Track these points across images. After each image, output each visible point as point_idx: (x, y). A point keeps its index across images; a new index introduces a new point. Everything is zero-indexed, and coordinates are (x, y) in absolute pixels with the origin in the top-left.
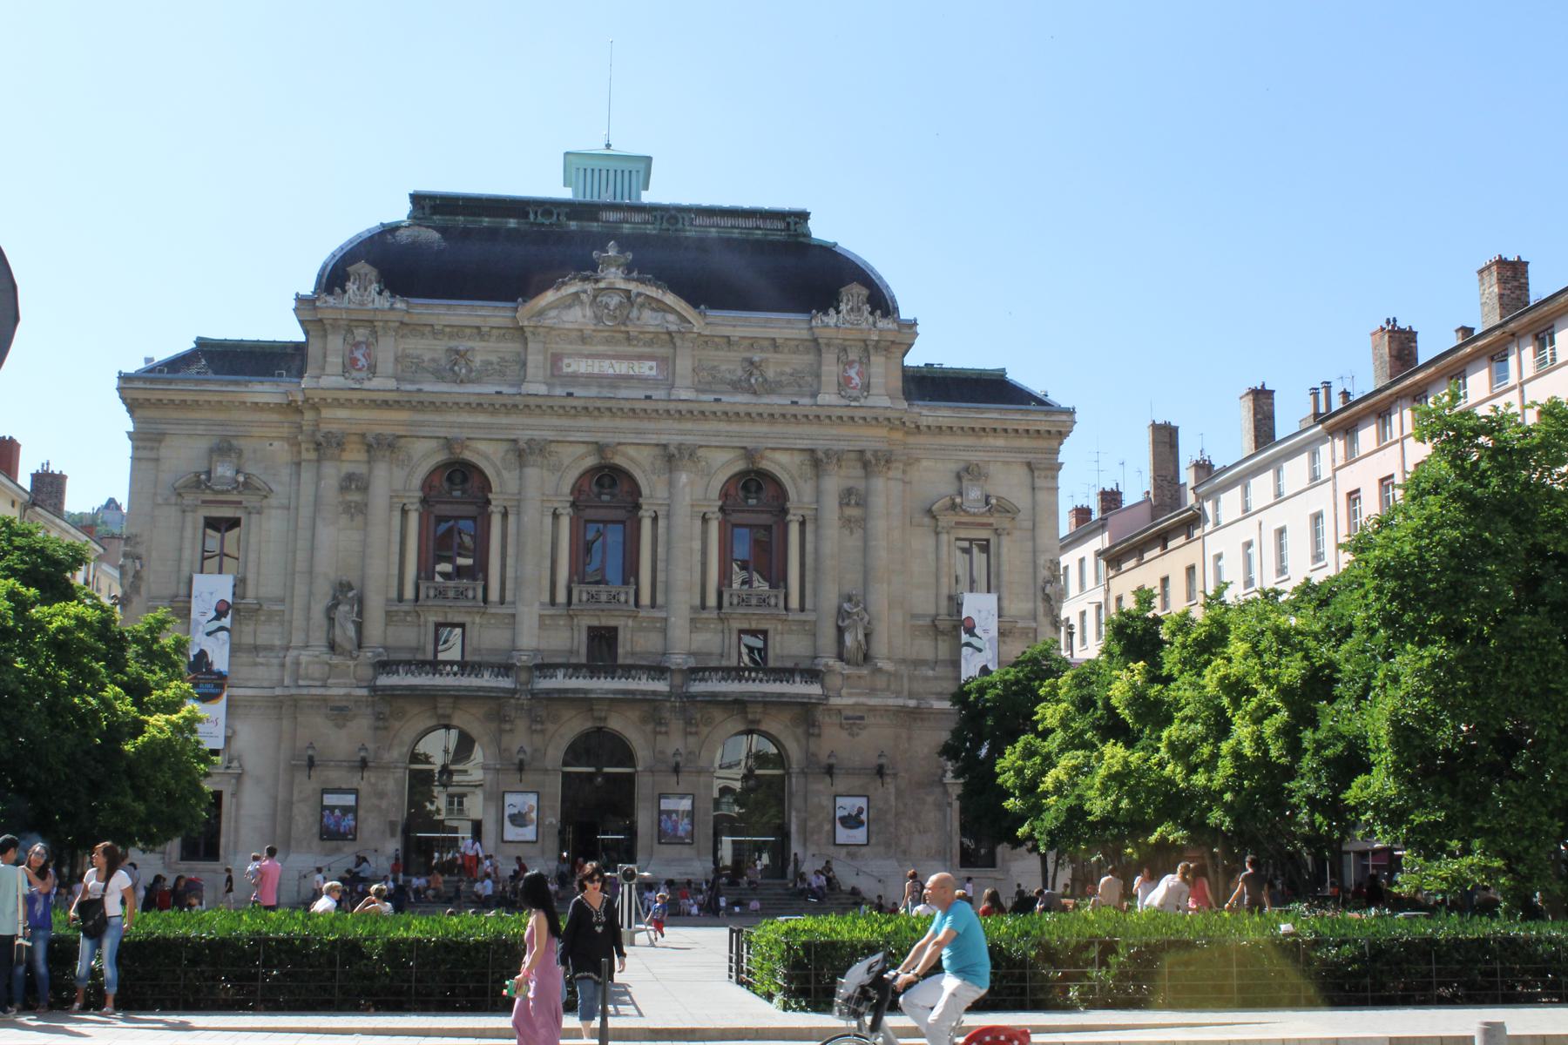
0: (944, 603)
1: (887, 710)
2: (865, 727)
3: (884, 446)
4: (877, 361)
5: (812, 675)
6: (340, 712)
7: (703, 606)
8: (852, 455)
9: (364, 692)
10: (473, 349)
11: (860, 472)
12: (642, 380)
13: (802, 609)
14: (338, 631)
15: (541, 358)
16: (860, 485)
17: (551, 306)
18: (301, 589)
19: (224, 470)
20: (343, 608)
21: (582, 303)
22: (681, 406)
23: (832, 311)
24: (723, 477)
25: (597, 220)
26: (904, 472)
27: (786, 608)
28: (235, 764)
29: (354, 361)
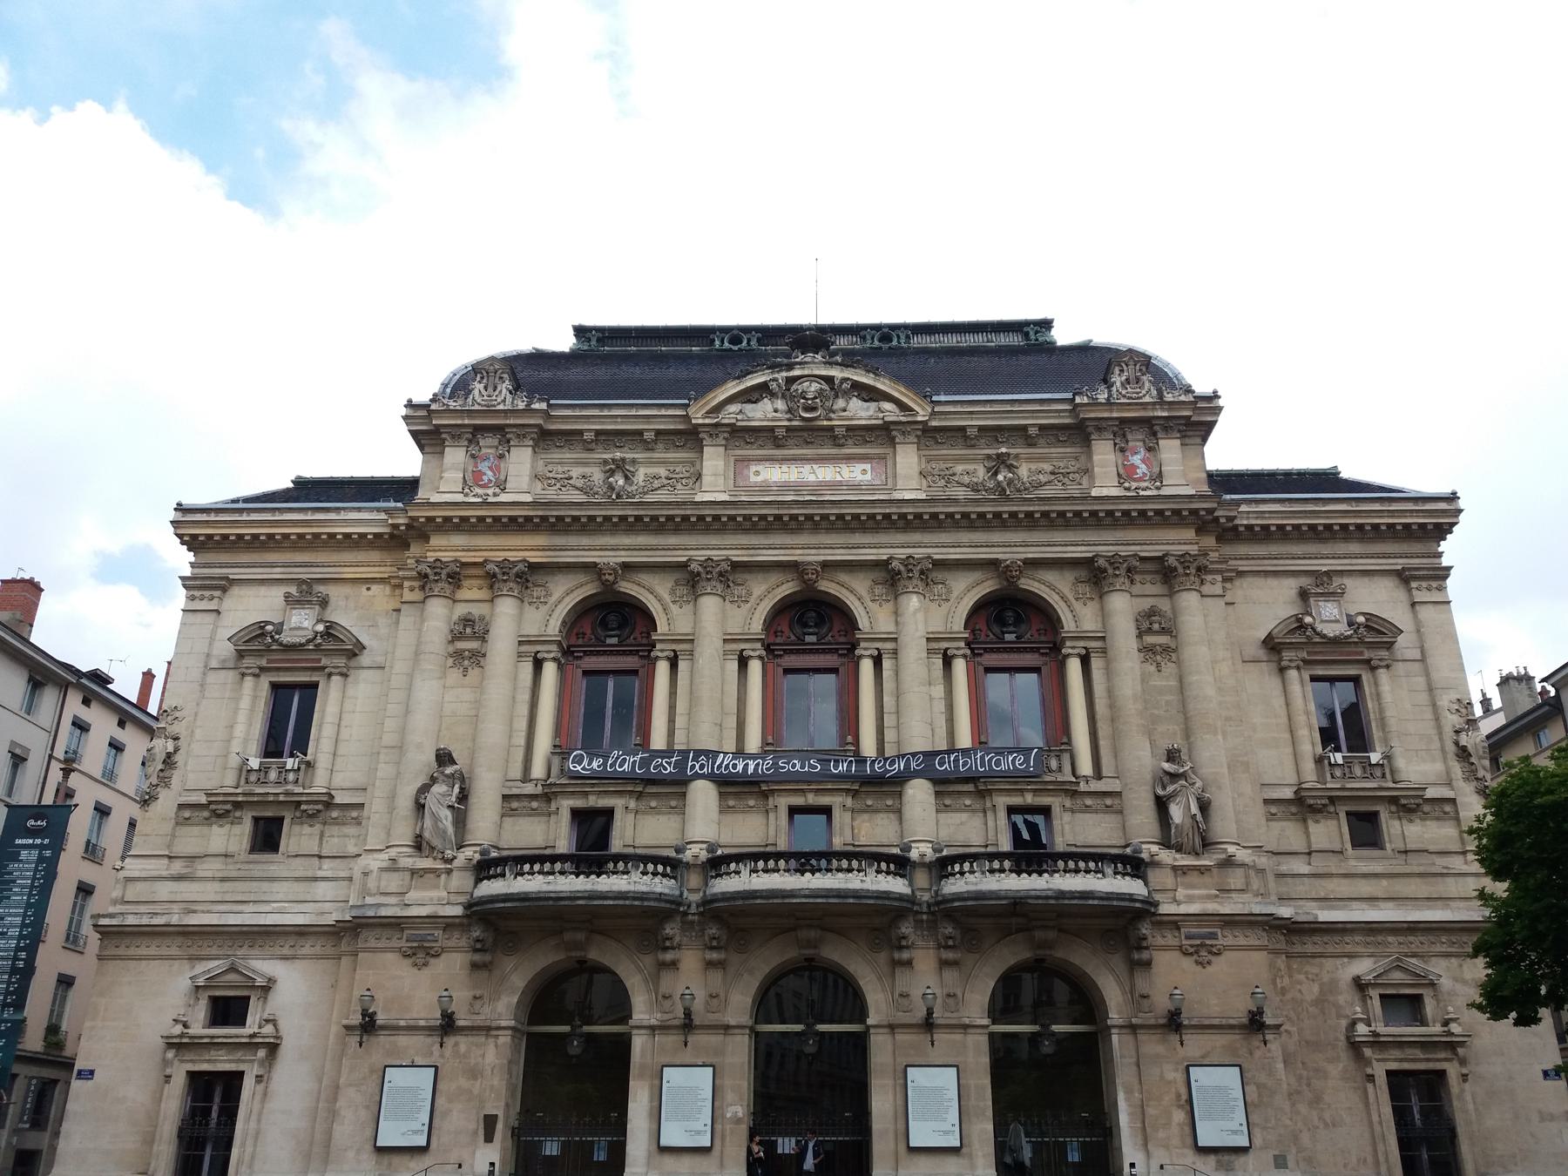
0: (1309, 767)
3: (1193, 549)
8: (1149, 566)
9: (458, 911)
10: (634, 461)
12: (855, 487)
13: (1098, 775)
14: (428, 822)
16: (1164, 605)
17: (731, 400)
18: (385, 770)
20: (439, 789)
29: (478, 475)
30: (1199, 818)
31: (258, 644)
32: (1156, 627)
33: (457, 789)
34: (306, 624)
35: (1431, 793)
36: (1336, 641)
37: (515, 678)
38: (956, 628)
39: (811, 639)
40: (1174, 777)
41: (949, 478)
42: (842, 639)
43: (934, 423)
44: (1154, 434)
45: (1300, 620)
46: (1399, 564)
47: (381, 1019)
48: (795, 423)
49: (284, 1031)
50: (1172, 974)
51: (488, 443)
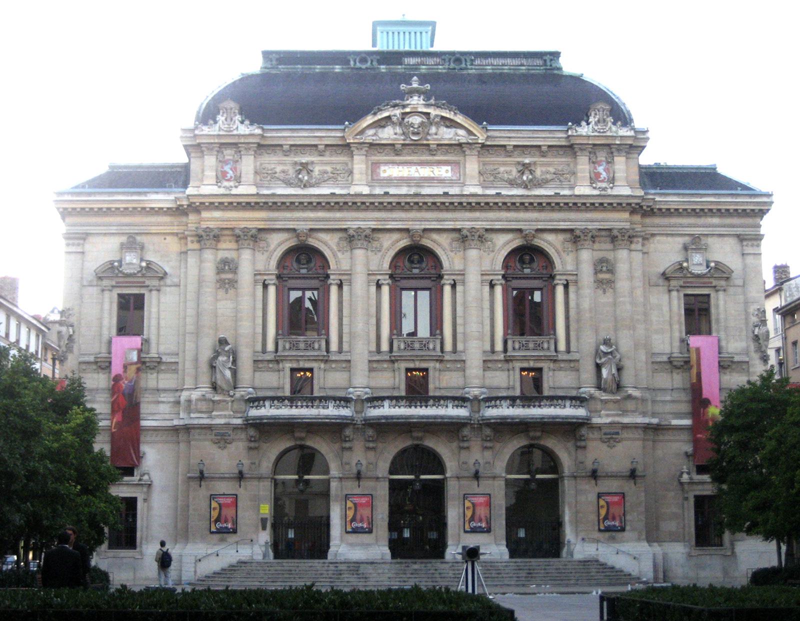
0: (677, 344)
1: (636, 426)
2: (619, 442)
3: (627, 225)
5: (579, 400)
6: (221, 436)
7: (493, 351)
8: (603, 233)
9: (239, 421)
10: (312, 163)
12: (441, 181)
13: (568, 351)
14: (218, 376)
15: (363, 166)
16: (610, 256)
17: (369, 127)
19: (131, 258)
20: (222, 359)
21: (393, 123)
23: (583, 123)
24: (505, 252)
25: (401, 64)
26: (643, 245)
27: (556, 350)
28: (146, 477)
29: (224, 174)
30: (616, 375)
31: (111, 272)
32: (604, 269)
33: (231, 358)
34: (134, 261)
35: (737, 359)
36: (698, 276)
37: (254, 295)
38: (497, 268)
40: (606, 354)
41: (495, 175)
42: (433, 271)
43: (488, 143)
44: (612, 153)
45: (681, 264)
46: (739, 231)
47: (205, 472)
48: (407, 142)
49: (153, 479)
50: (597, 452)
51: (229, 153)
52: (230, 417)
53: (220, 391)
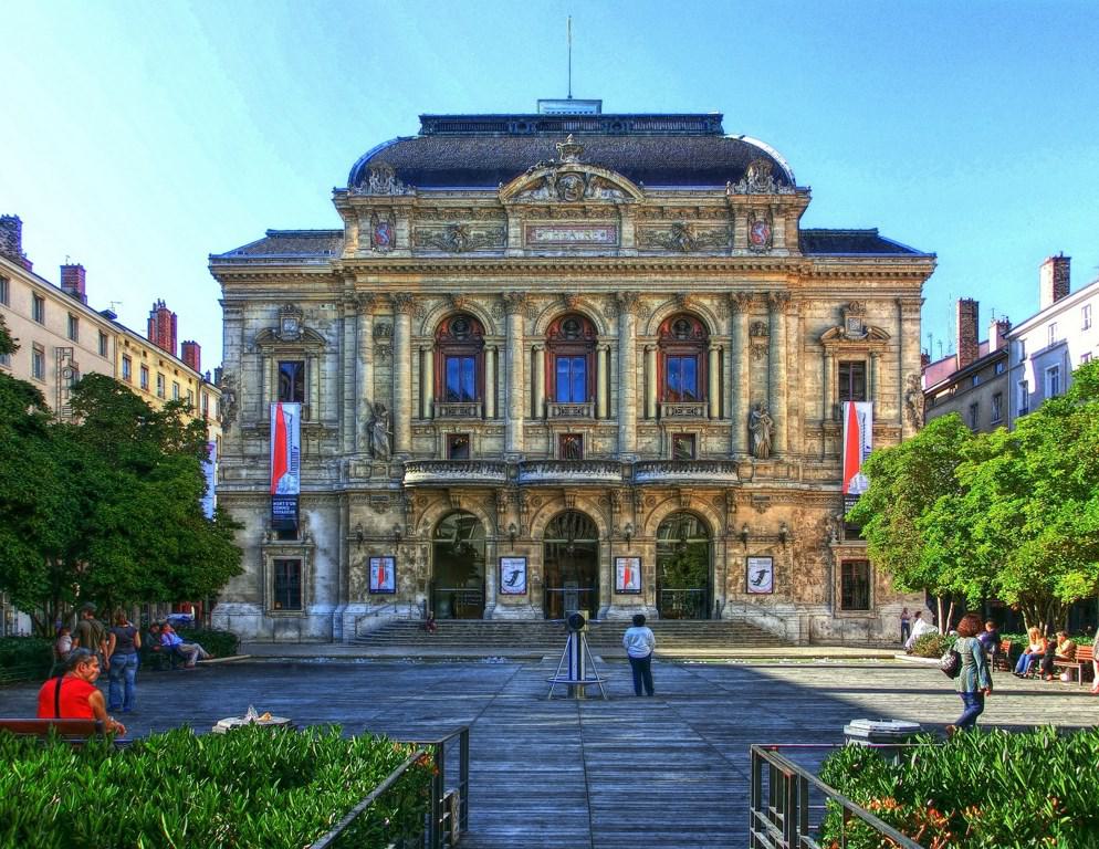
2: (770, 506)
4: (779, 225)
6: (379, 502)
7: (646, 417)
11: (764, 311)
14: (376, 441)
16: (764, 320)
19: (289, 325)
21: (548, 184)
22: (628, 262)
23: (742, 182)
24: (659, 318)
26: (800, 311)
28: (309, 541)
29: (378, 237)
39: (571, 337)
45: (838, 330)
52: (387, 481)
53: (376, 456)
